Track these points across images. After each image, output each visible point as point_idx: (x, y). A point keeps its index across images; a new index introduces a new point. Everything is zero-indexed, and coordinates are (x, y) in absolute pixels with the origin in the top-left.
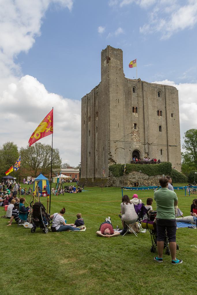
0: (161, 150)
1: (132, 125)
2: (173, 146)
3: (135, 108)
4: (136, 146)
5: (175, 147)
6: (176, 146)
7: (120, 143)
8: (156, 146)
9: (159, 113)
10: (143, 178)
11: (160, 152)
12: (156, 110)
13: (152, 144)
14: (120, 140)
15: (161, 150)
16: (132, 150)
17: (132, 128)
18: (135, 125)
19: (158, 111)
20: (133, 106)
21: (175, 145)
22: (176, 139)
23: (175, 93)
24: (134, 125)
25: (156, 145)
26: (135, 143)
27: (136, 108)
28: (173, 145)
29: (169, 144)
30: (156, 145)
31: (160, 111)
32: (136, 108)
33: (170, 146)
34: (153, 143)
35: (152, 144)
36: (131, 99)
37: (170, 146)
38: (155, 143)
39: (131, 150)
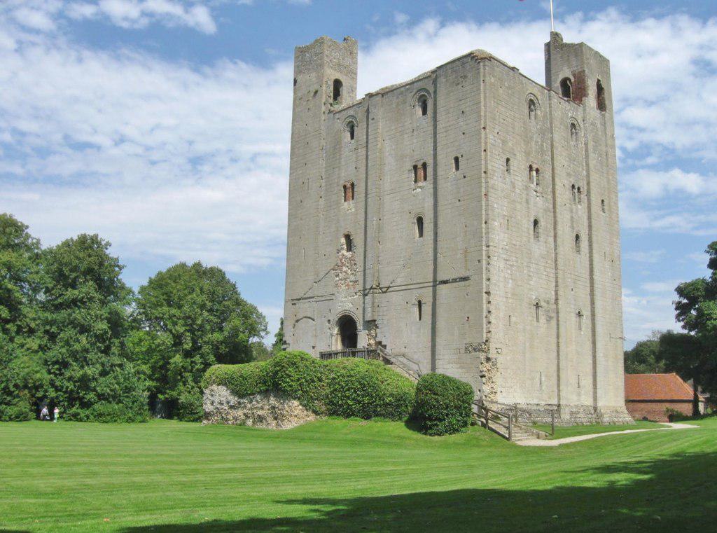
0: (420, 302)
1: (338, 239)
2: (455, 280)
3: (348, 185)
4: (347, 303)
5: (463, 283)
6: (465, 279)
7: (305, 303)
8: (402, 293)
9: (420, 170)
10: (228, 403)
11: (417, 309)
12: (409, 166)
13: (389, 287)
14: (306, 296)
15: (420, 302)
16: (334, 318)
17: (338, 251)
18: (348, 237)
19: (415, 167)
20: (342, 182)
21: (463, 274)
22: (466, 252)
23: (469, 75)
24: (343, 240)
25: (403, 288)
26: (341, 297)
27: (353, 185)
28: (456, 275)
29: (441, 277)
30: (403, 288)
31: (419, 166)
32: (353, 185)
33: (445, 282)
34: (394, 284)
35: (389, 287)
36: (340, 163)
37: (445, 282)
38: (399, 282)
39: (331, 319)
